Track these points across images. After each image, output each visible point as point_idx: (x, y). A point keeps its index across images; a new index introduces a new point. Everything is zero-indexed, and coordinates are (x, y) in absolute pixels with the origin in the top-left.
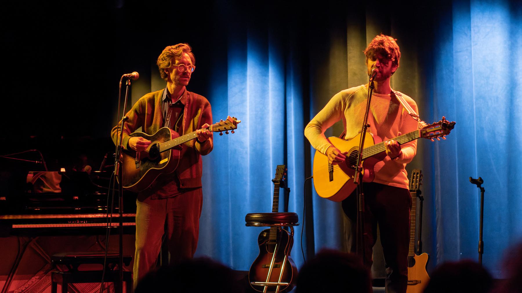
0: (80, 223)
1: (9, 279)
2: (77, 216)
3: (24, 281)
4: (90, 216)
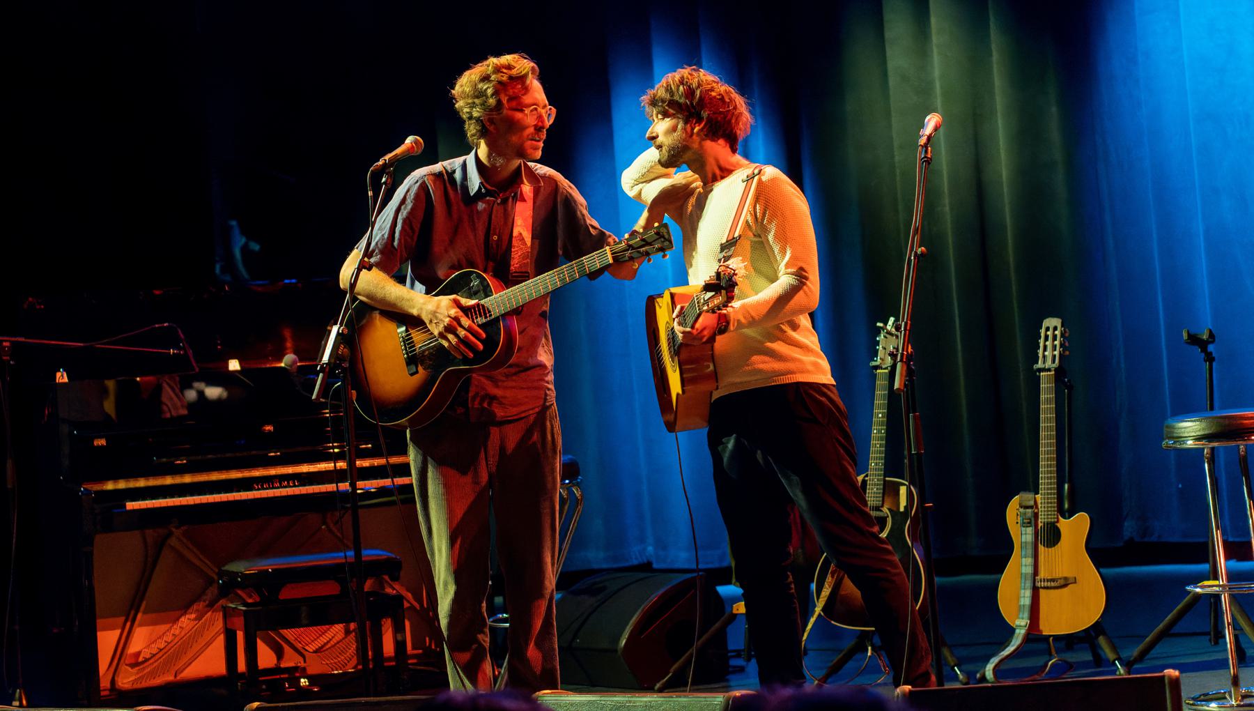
0: (281, 487)
1: (128, 624)
2: (273, 472)
3: (163, 628)
4: (305, 468)
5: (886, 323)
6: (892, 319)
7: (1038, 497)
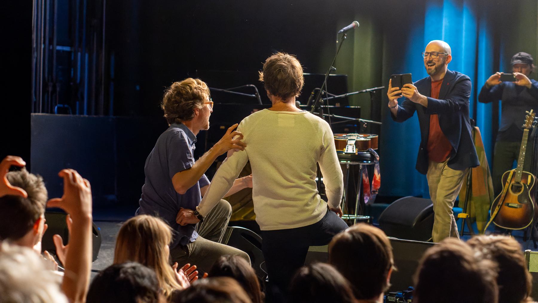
5: (530, 112)
6: (532, 111)
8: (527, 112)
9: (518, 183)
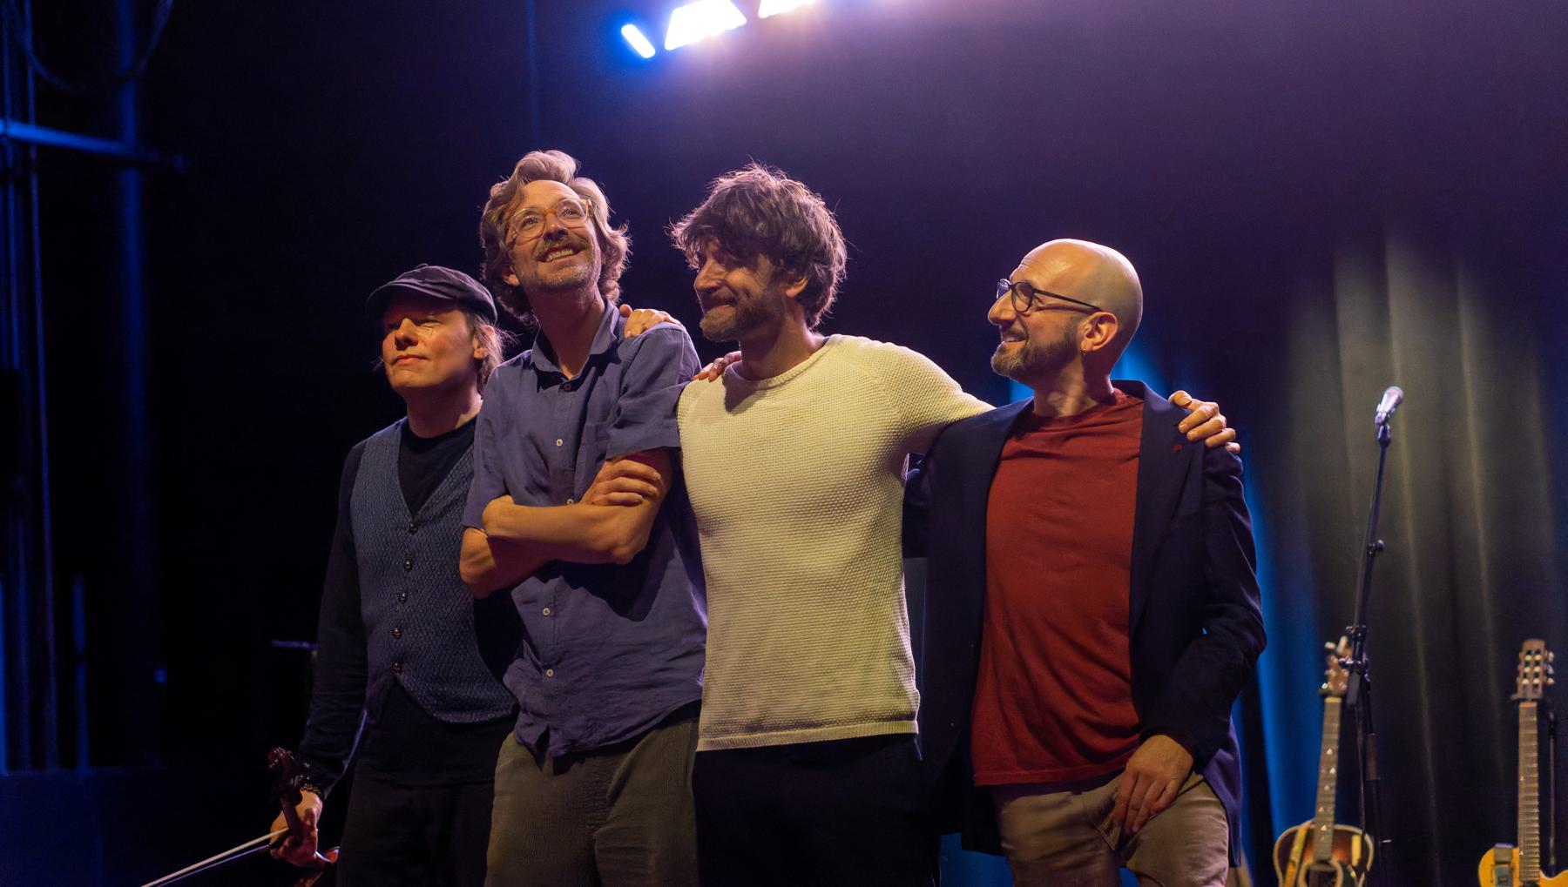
5: (1337, 643)
6: (1343, 641)
7: (1516, 850)
8: (1330, 645)
9: (1325, 862)
